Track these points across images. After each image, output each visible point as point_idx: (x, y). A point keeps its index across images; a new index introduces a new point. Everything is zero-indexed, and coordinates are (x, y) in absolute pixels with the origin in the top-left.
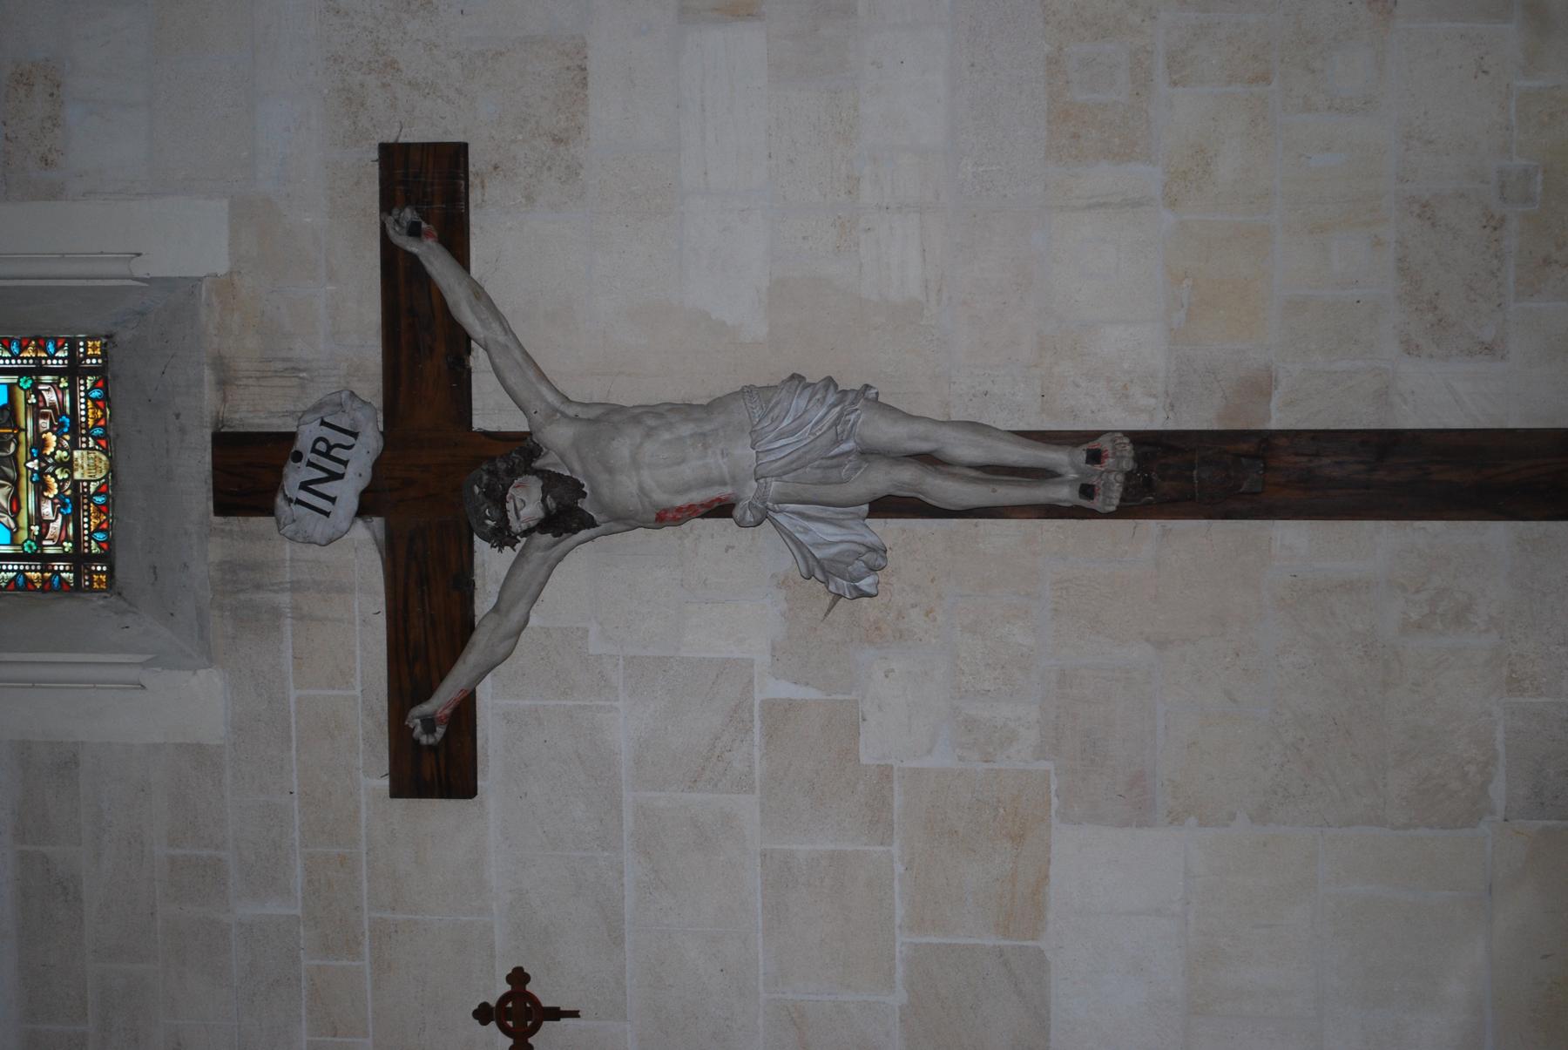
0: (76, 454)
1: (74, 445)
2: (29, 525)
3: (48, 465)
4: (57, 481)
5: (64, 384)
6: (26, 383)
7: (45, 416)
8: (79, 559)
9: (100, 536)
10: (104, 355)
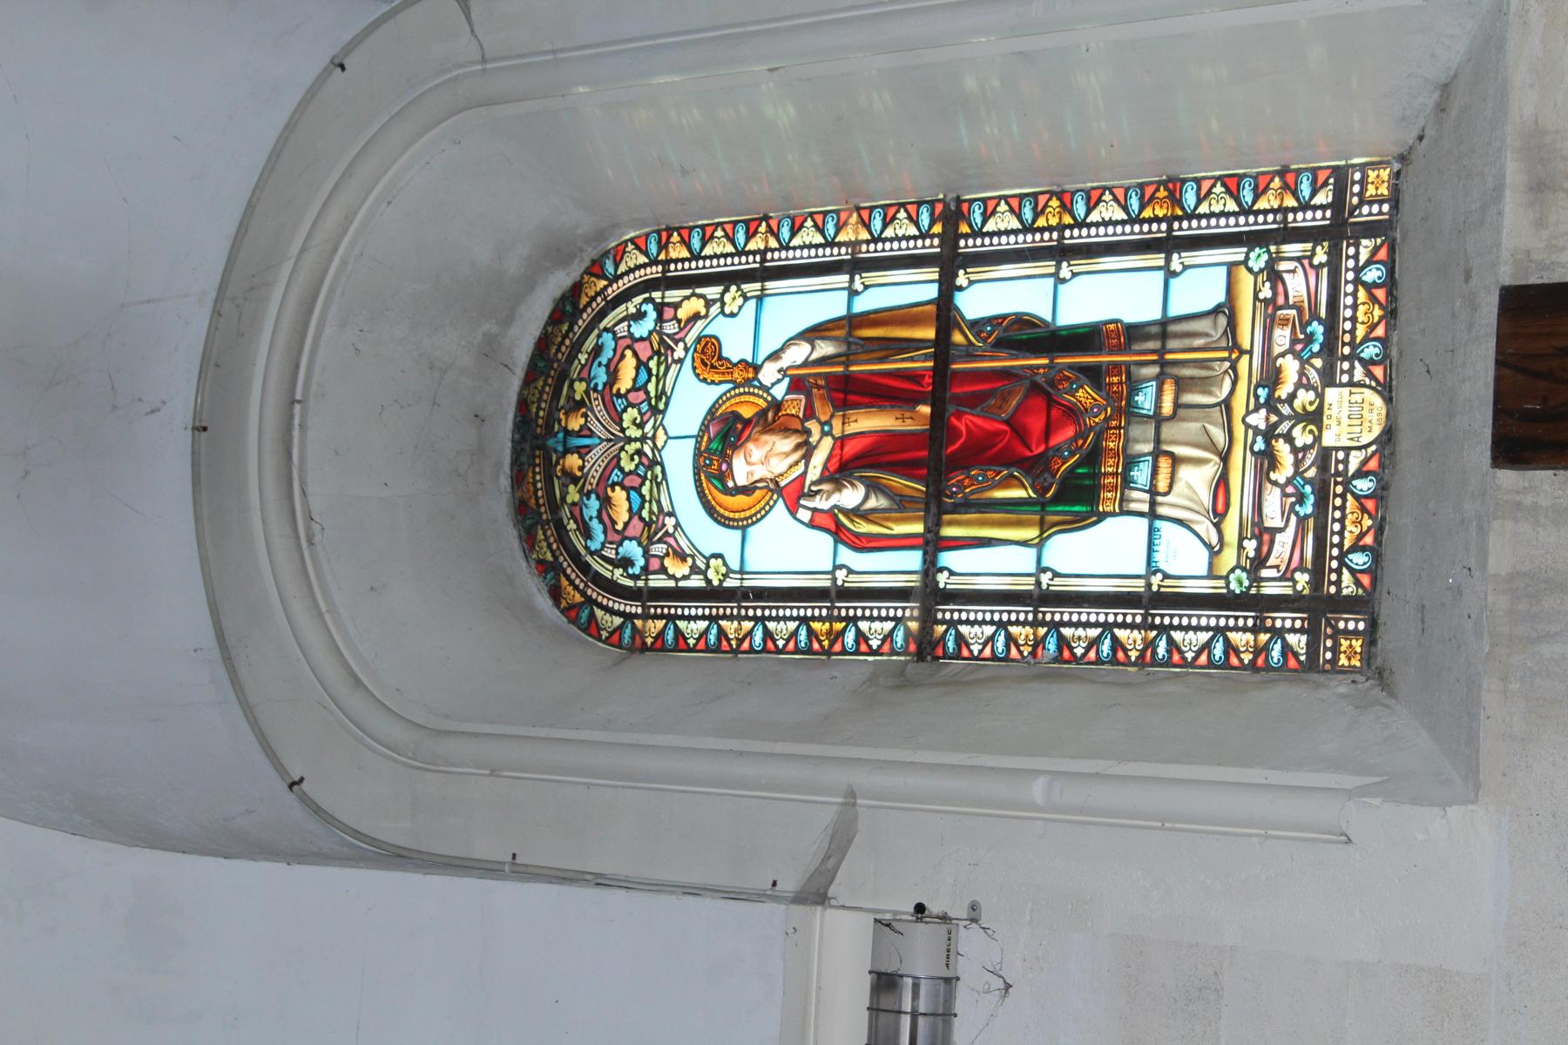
0: (1331, 394)
1: (1329, 378)
2: (1241, 539)
3: (1282, 418)
4: (1295, 450)
5: (1321, 257)
6: (1258, 259)
7: (1285, 322)
8: (1319, 607)
9: (1359, 560)
10: (1395, 199)
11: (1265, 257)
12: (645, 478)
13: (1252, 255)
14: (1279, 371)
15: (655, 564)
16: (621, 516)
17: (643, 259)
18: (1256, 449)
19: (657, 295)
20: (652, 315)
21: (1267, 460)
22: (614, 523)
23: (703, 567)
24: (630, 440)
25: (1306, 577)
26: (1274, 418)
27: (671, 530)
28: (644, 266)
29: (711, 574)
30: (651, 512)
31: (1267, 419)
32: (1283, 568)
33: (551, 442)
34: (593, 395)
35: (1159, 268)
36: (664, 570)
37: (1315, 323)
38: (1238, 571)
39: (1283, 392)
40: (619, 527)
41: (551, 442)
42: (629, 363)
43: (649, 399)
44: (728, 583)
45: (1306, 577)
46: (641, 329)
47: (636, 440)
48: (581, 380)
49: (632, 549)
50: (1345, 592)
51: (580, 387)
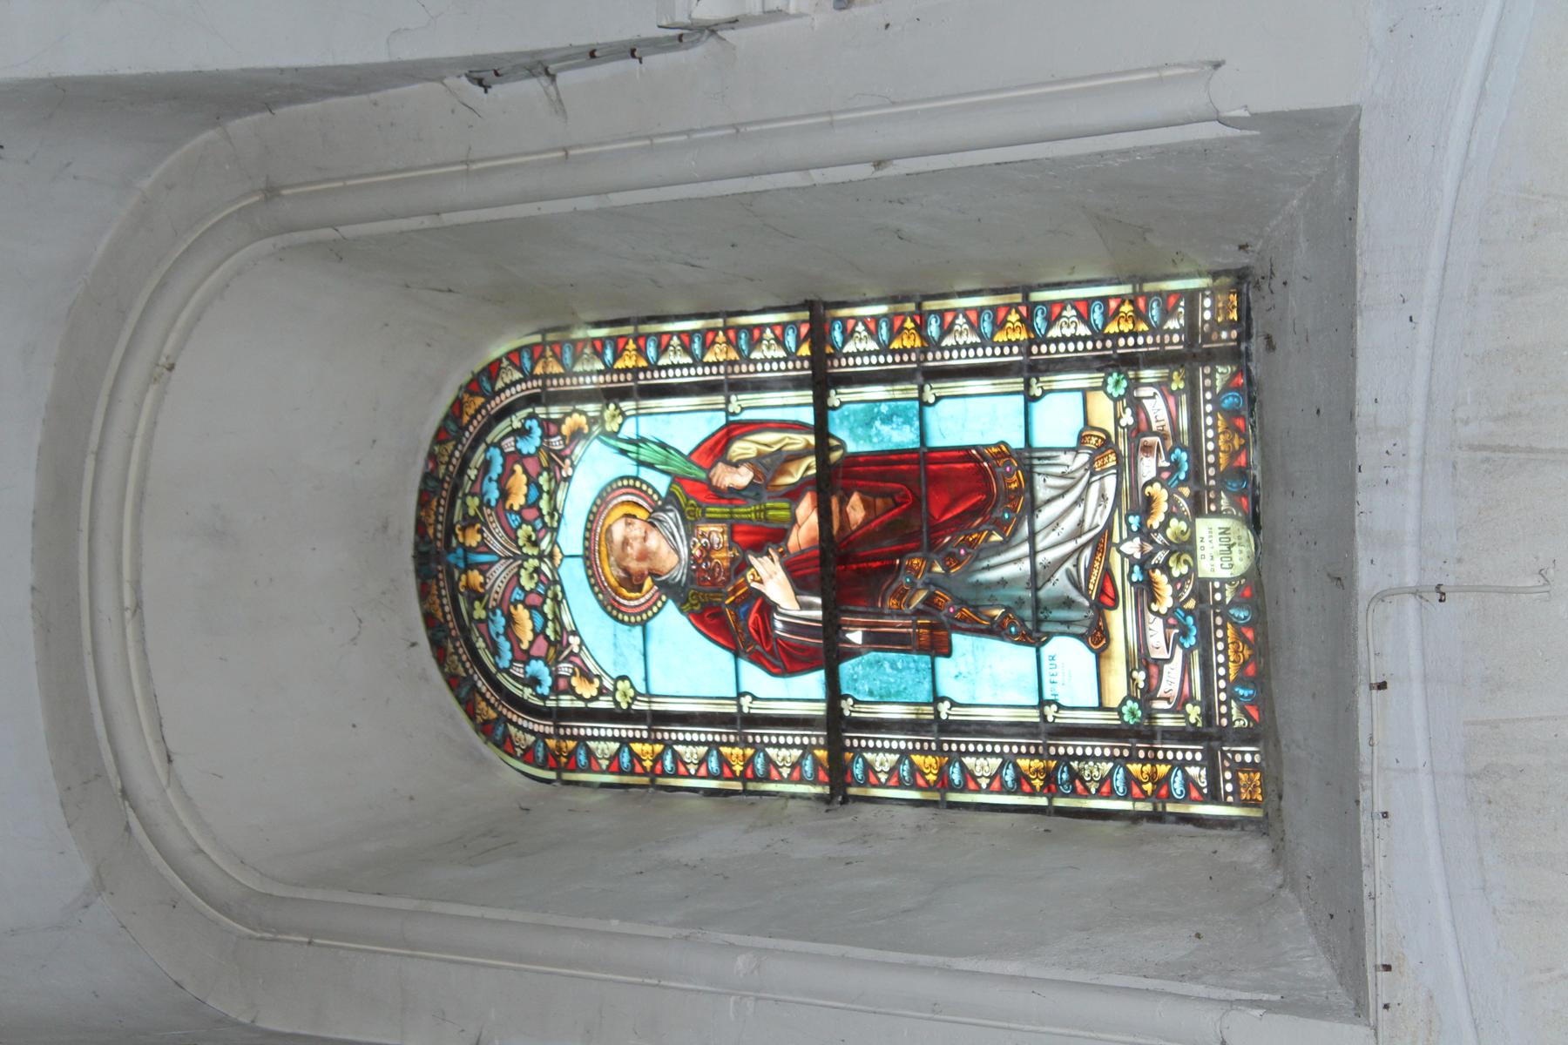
1: (1198, 509)
3: (1158, 548)
4: (1172, 580)
7: (1147, 449)
11: (1124, 384)
12: (546, 596)
13: (1111, 380)
14: (1150, 500)
15: (562, 684)
16: (526, 636)
17: (517, 375)
18: (1135, 578)
19: (540, 410)
20: (537, 432)
21: (1147, 591)
22: (520, 641)
23: (611, 688)
24: (527, 557)
25: (1198, 709)
26: (1149, 548)
27: (576, 650)
28: (519, 381)
29: (619, 697)
30: (555, 632)
31: (1142, 548)
32: (1173, 701)
33: (451, 558)
34: (487, 511)
35: (1017, 393)
36: (570, 690)
37: (1178, 451)
38: (1129, 703)
39: (1155, 522)
40: (525, 646)
41: (451, 558)
42: (519, 480)
43: (541, 516)
44: (637, 706)
45: (1198, 709)
46: (529, 446)
47: (533, 557)
48: (473, 495)
49: (537, 667)
50: (1237, 724)
51: (473, 503)
